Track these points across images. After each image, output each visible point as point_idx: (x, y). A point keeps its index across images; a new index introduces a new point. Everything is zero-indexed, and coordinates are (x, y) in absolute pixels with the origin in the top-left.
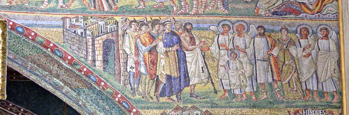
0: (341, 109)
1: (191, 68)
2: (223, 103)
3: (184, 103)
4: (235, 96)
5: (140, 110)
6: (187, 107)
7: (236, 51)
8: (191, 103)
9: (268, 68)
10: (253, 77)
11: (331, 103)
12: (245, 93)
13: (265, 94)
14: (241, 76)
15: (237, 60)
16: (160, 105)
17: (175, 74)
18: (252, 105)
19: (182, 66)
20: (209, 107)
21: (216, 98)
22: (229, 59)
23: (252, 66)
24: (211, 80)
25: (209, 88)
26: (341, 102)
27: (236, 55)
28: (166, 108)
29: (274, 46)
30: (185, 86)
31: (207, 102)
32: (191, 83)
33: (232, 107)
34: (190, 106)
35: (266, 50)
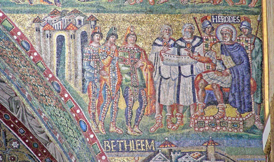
0: (259, 16)
3: (63, 5)
5: (7, 14)
6: (66, 11)
8: (73, 6)
11: (248, 8)
16: (32, 8)
26: (260, 7)
28: (41, 12)
31: (91, 6)
33: (123, 12)
34: (70, 9)
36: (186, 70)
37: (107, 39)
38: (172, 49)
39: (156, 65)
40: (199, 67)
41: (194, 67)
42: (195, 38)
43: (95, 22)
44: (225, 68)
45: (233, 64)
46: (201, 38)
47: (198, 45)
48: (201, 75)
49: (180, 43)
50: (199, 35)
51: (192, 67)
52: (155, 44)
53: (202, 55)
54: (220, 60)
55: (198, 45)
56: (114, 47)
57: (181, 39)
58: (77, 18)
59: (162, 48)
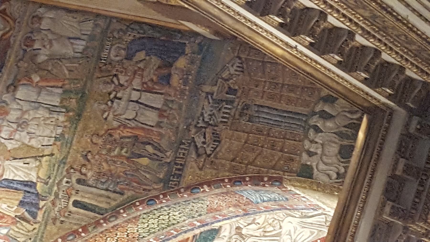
1: (21, 176)
2: (65, 150)
4: (62, 135)
7: (21, 122)
8: (53, 186)
9: (48, 91)
10: (51, 109)
12: (63, 122)
13: (71, 100)
14: (47, 122)
15: (30, 123)
17: (20, 196)
18: (77, 118)
19: (15, 186)
20: (64, 168)
21: (58, 156)
22: (26, 131)
23: (41, 108)
24: (39, 156)
25: (46, 161)
27: (24, 122)
29: (30, 78)
30: (35, 188)
32: (35, 181)
35: (30, 88)
36: (135, 95)
37: (88, 161)
38: (115, 104)
39: (122, 122)
40: (136, 83)
41: (135, 88)
42: (113, 82)
43: (72, 168)
44: (144, 59)
45: (144, 52)
46: (115, 75)
47: (118, 80)
48: (144, 83)
49: (112, 96)
50: (111, 77)
51: (134, 89)
52: (106, 119)
53: (127, 78)
54: (137, 62)
55: (118, 80)
56: (97, 157)
57: (110, 94)
58: (64, 184)
59: (111, 113)
